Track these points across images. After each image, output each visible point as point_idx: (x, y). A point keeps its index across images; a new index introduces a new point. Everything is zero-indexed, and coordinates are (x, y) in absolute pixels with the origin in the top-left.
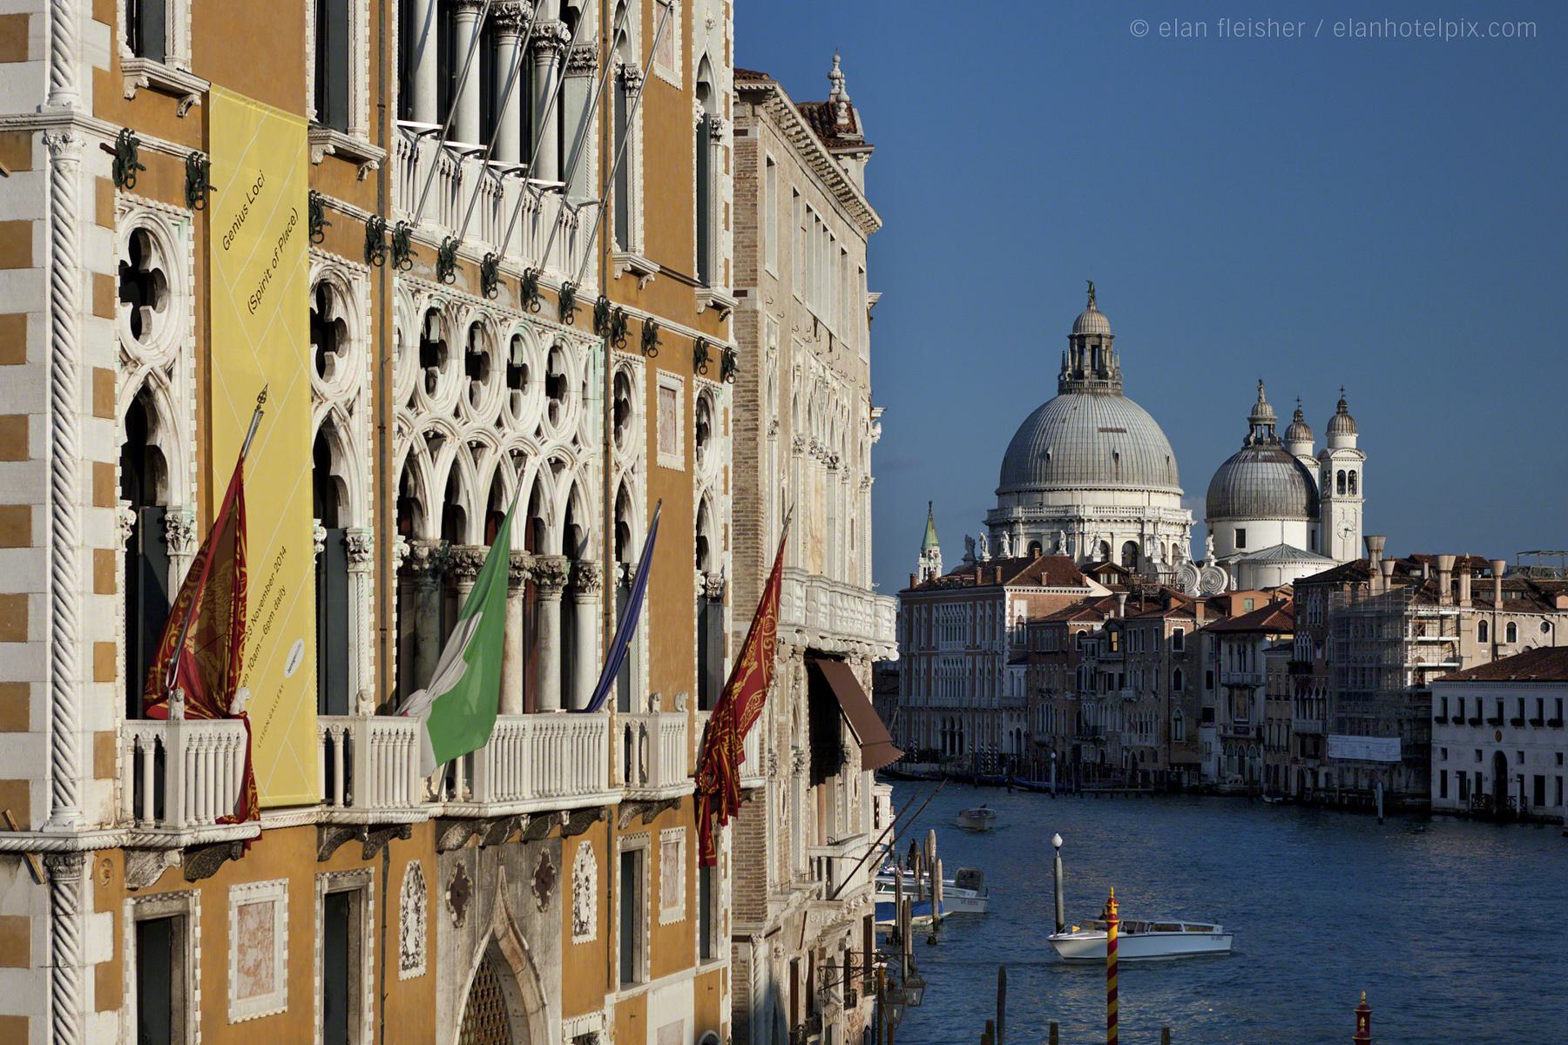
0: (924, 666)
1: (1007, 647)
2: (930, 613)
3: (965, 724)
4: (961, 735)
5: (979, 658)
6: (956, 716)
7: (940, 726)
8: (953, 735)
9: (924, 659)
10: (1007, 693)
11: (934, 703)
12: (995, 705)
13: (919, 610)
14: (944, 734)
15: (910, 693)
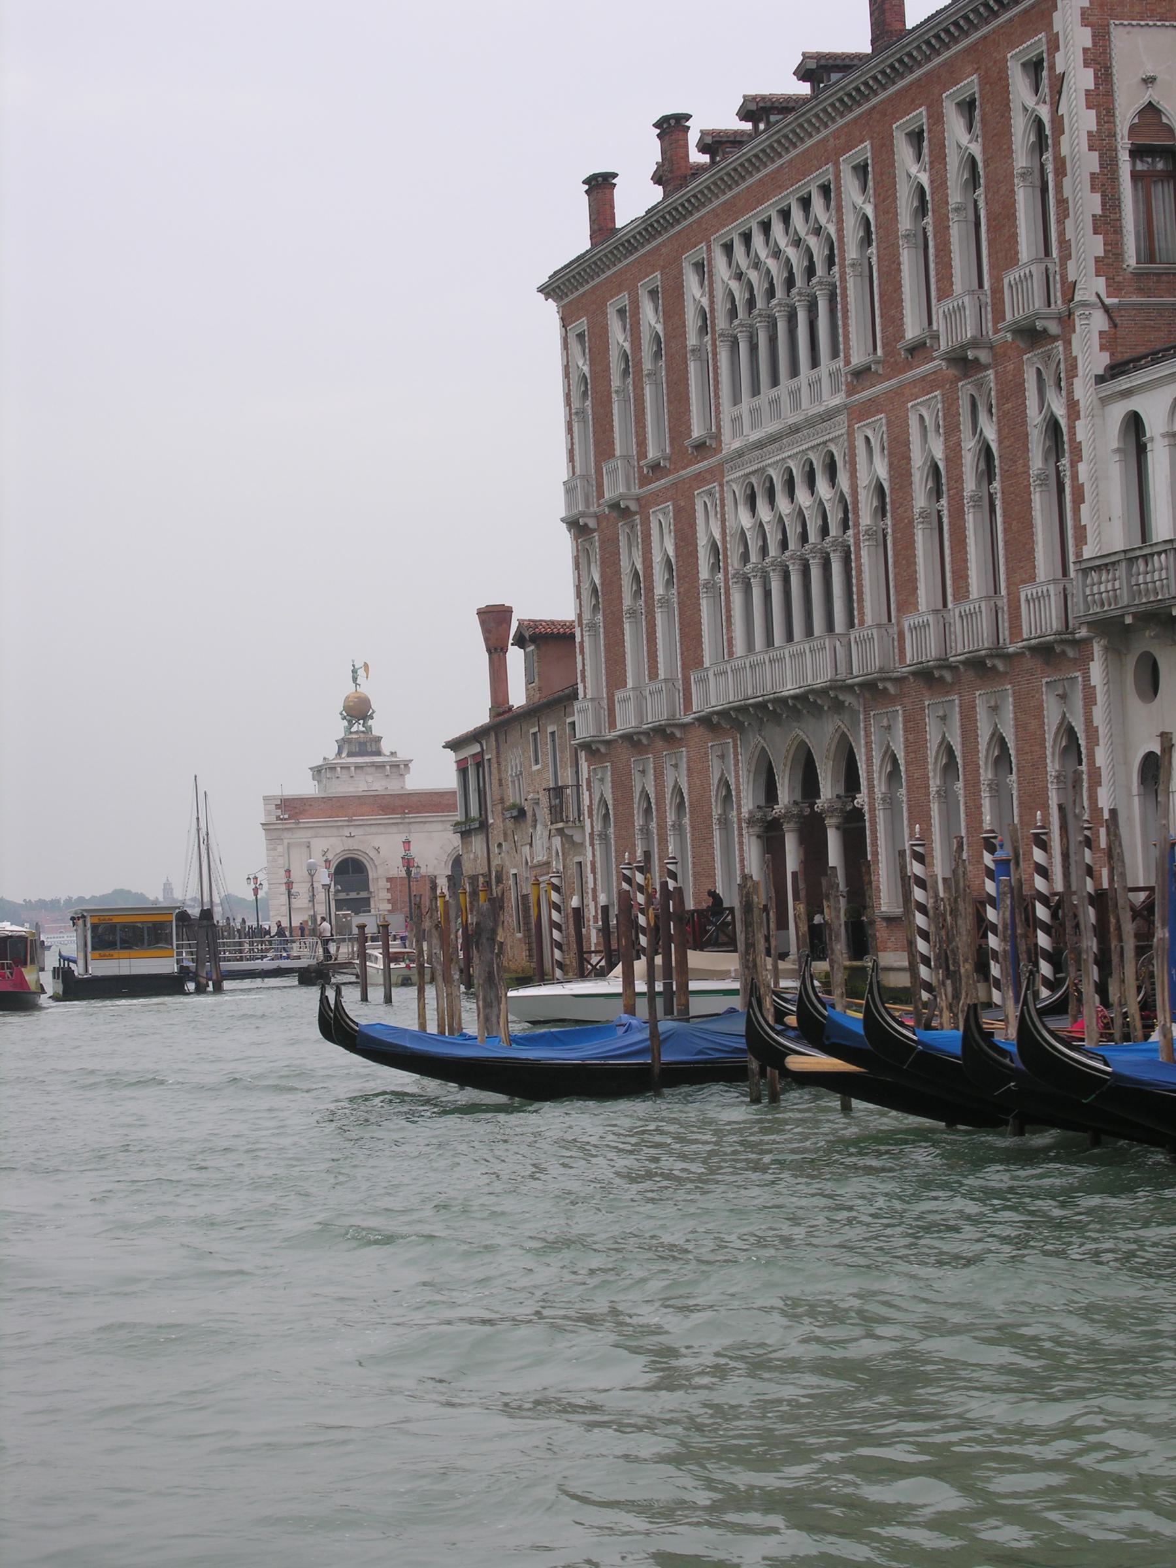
0: (665, 545)
1: (1091, 286)
2: (670, 300)
3: (872, 772)
4: (854, 829)
5: (924, 411)
6: (821, 737)
7: (747, 801)
8: (819, 833)
9: (661, 520)
10: (1108, 532)
11: (716, 693)
12: (1041, 619)
13: (630, 316)
14: (771, 835)
15: (616, 678)
